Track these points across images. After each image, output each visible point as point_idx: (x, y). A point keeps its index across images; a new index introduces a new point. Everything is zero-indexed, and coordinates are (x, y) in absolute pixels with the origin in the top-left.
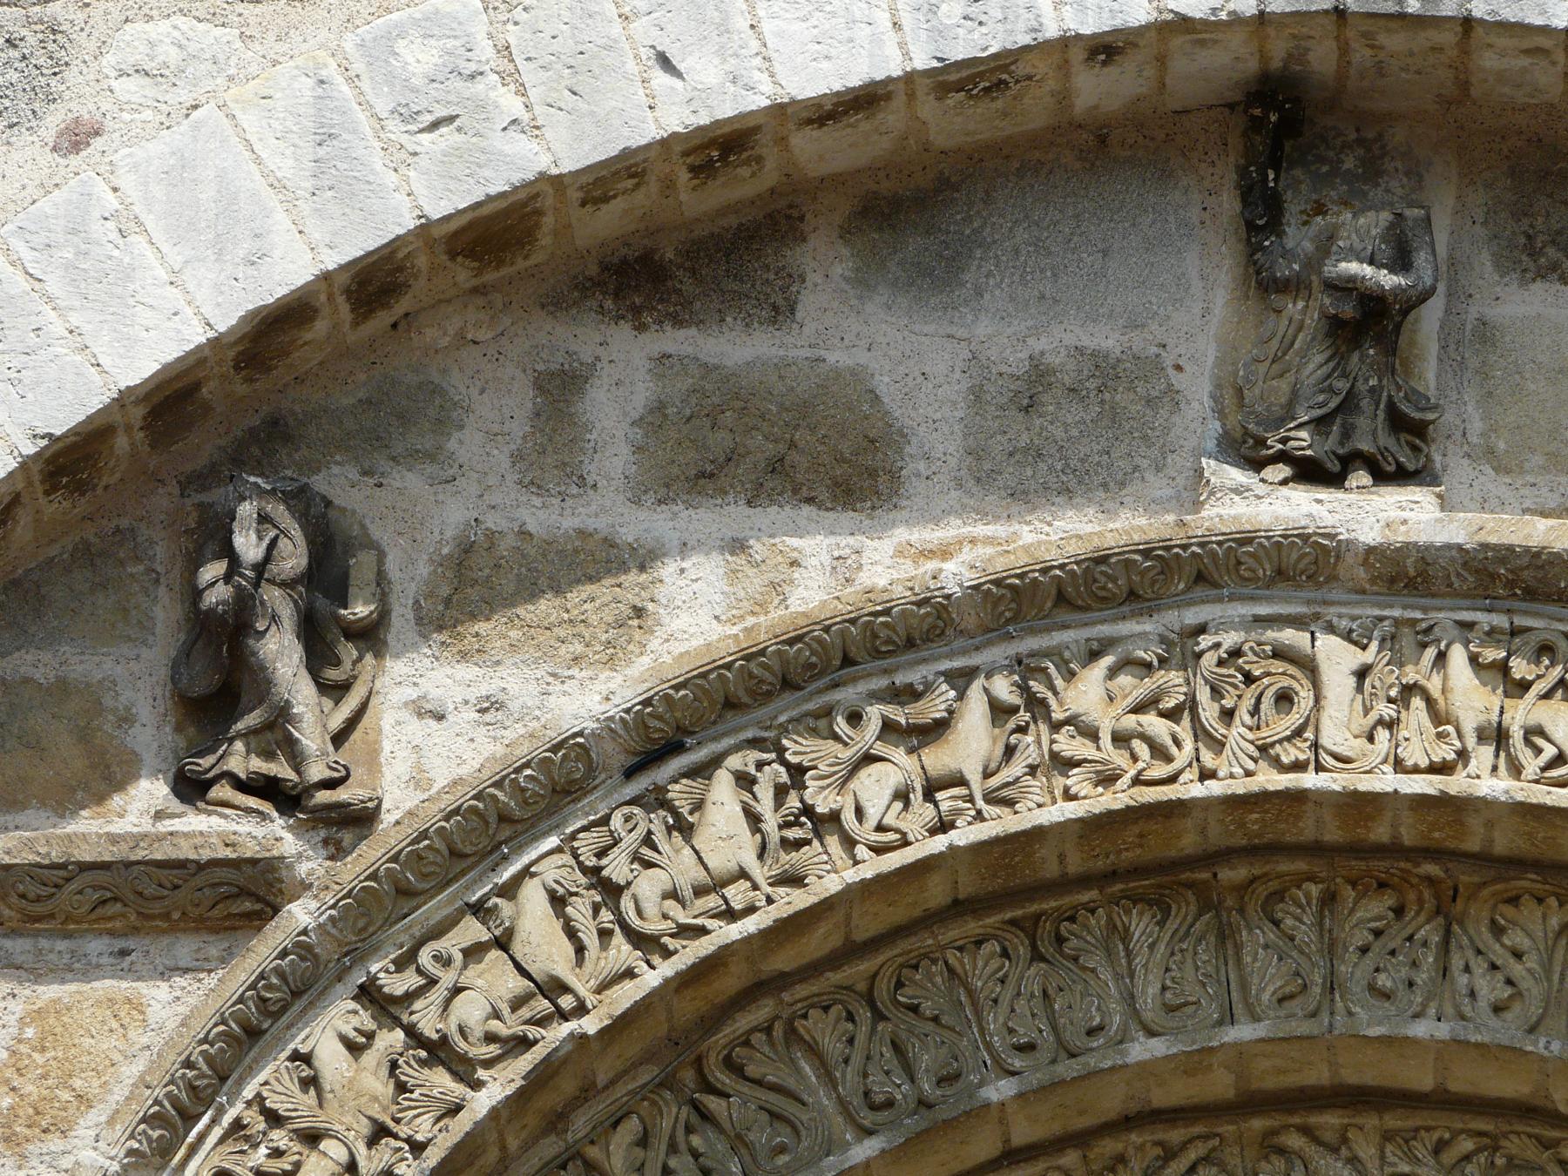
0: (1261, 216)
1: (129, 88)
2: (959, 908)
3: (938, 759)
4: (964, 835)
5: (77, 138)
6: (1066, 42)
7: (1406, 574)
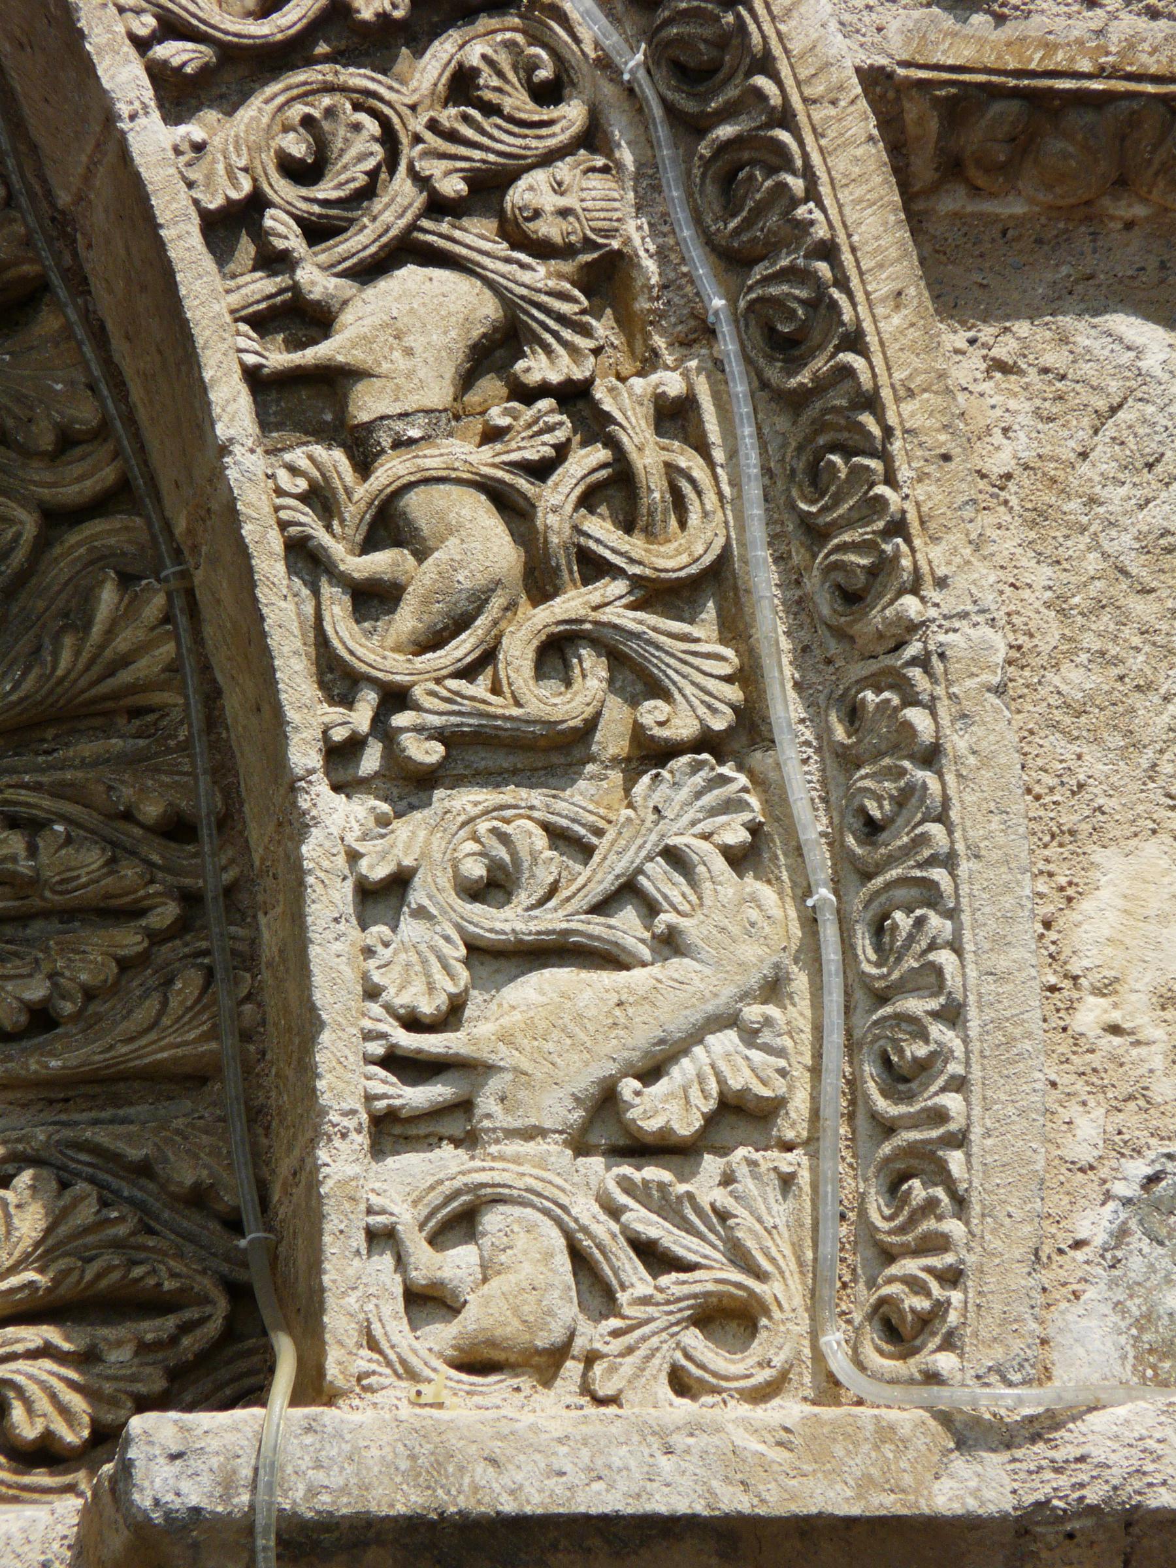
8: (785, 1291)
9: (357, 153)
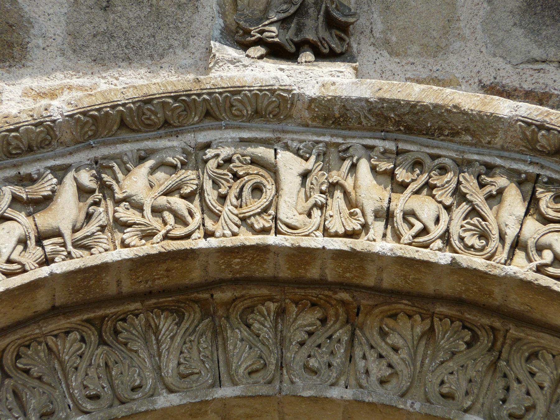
2: (55, 311)
4: (60, 267)
7: (334, 115)
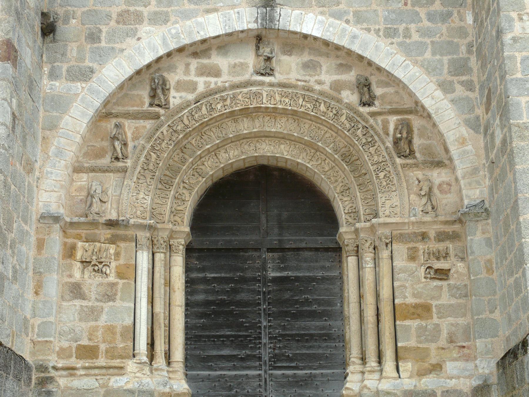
0: (258, 48)
1: (144, 34)
3: (225, 103)
4: (227, 111)
5: (139, 39)
6: (238, 31)
7: (271, 85)
8: (399, 213)
9: (380, 168)
